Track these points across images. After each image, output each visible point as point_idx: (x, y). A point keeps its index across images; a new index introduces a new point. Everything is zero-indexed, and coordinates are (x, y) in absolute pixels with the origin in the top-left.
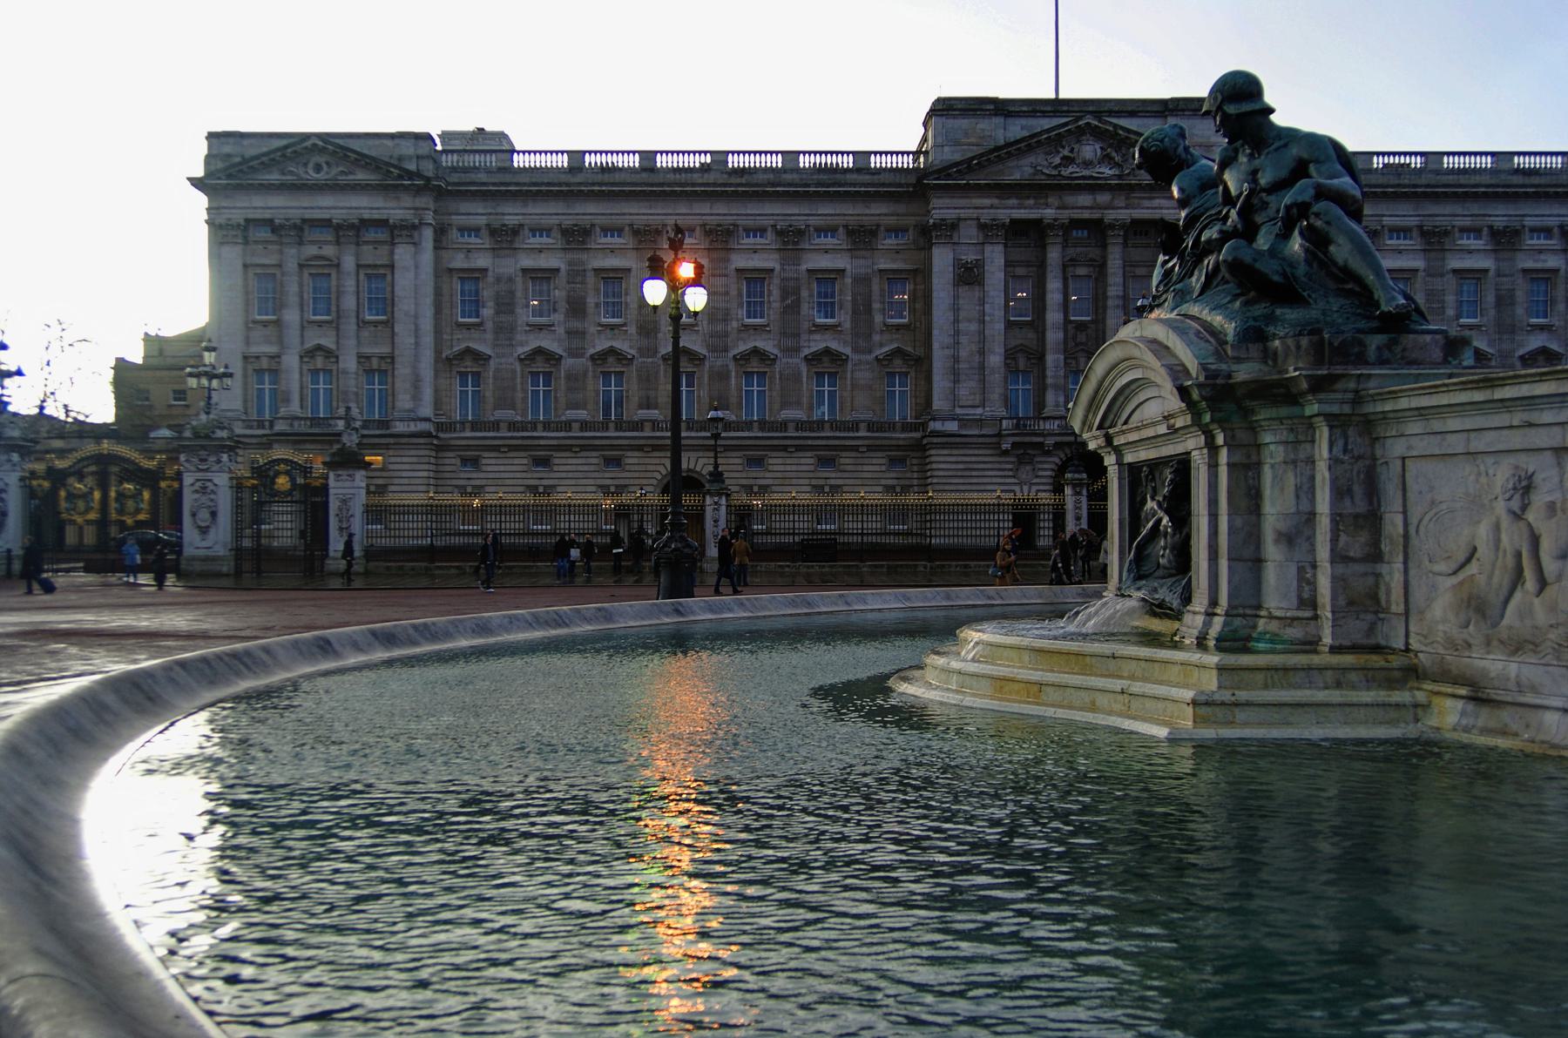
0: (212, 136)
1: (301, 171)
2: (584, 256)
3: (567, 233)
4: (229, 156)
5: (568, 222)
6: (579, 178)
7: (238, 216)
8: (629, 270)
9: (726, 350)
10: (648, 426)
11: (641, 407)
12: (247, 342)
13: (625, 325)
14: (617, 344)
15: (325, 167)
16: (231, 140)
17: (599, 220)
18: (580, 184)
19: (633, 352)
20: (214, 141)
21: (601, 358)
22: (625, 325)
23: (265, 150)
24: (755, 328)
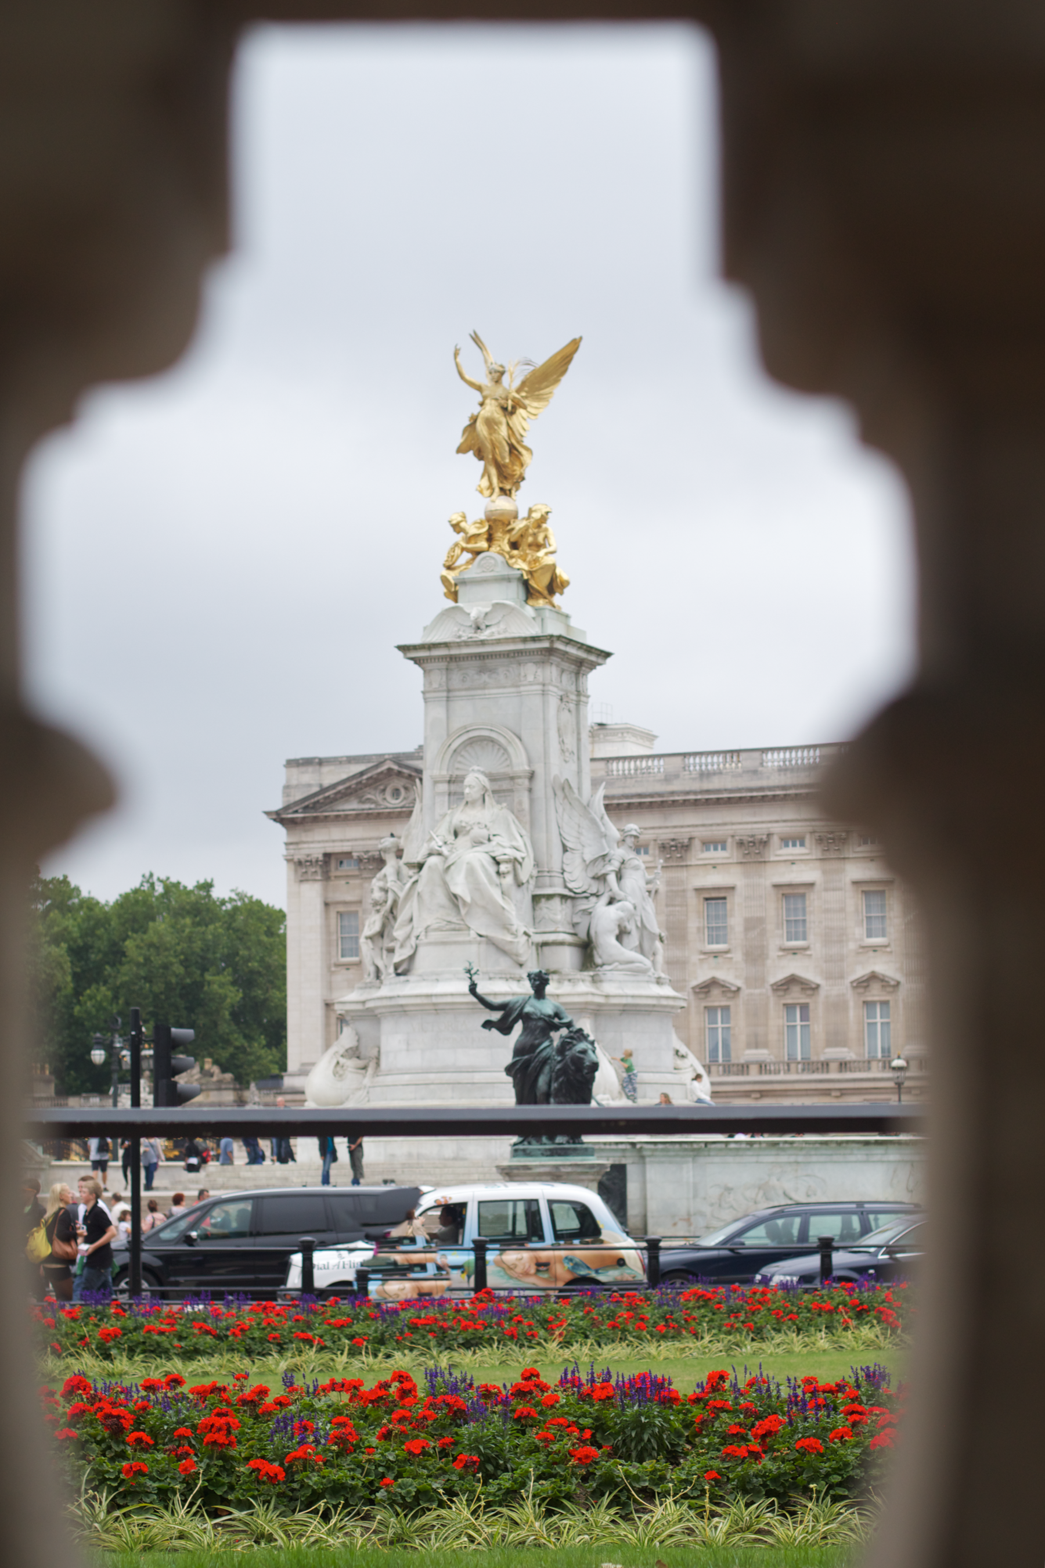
0: (291, 763)
1: (379, 798)
2: (683, 874)
3: (663, 847)
4: (309, 785)
5: (665, 835)
6: (676, 786)
7: (316, 851)
8: (732, 888)
9: (842, 977)
10: (754, 1069)
11: (749, 1046)
12: (330, 987)
13: (727, 952)
14: (721, 975)
15: (403, 791)
16: (310, 769)
17: (698, 833)
18: (672, 793)
19: (739, 983)
20: (294, 771)
21: (707, 988)
22: (727, 952)
23: (344, 776)
24: (875, 949)
